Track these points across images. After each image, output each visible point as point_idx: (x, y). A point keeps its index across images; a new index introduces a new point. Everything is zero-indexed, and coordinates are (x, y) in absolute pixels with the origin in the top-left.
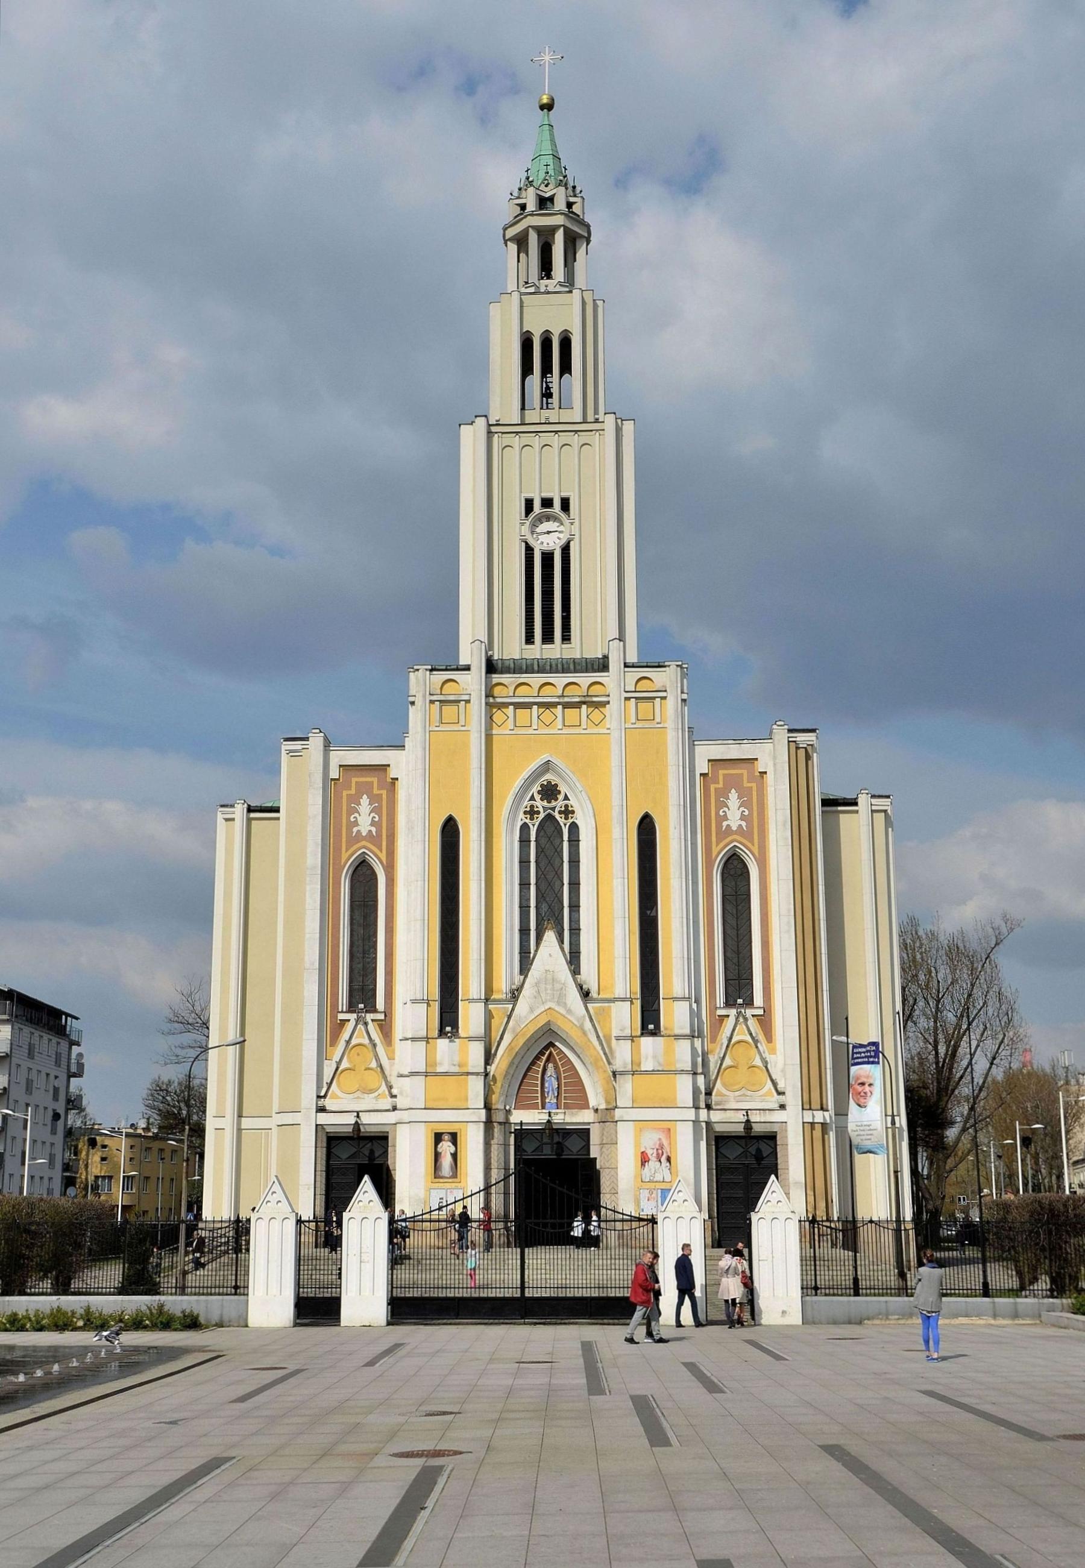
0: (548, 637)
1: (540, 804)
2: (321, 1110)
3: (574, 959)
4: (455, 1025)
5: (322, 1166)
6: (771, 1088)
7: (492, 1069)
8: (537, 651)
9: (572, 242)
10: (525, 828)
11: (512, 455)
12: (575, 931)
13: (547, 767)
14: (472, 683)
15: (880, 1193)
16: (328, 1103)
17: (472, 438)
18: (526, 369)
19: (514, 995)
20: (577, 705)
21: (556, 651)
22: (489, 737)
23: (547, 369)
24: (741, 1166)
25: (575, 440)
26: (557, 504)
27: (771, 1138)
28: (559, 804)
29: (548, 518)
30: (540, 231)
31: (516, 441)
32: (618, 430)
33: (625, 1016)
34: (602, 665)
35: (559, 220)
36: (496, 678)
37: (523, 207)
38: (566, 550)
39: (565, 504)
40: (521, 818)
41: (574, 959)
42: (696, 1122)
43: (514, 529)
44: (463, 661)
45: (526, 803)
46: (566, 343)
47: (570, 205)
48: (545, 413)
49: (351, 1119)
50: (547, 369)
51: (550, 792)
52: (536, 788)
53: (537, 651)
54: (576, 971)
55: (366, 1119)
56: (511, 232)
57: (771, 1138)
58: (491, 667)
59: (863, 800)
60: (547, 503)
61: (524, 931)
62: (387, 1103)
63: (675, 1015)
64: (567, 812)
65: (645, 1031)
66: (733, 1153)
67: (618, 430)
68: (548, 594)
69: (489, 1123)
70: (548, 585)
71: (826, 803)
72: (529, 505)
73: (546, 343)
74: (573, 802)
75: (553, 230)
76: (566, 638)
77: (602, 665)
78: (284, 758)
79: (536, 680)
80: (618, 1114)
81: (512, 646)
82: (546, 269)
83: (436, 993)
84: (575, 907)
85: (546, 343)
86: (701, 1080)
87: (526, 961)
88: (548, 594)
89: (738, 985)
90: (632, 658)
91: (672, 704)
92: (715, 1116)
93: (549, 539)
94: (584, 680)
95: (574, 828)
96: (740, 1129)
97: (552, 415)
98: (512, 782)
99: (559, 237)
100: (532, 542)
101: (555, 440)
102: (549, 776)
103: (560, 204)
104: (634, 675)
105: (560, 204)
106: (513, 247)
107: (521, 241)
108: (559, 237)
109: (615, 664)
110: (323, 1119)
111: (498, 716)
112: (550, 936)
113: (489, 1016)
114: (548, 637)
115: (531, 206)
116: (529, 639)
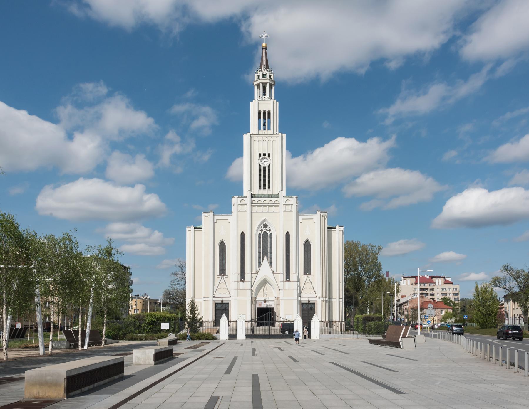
0: (265, 188)
1: (263, 229)
2: (214, 297)
3: (271, 264)
4: (244, 279)
5: (214, 309)
6: (313, 290)
7: (252, 288)
8: (262, 192)
9: (271, 86)
10: (260, 234)
11: (256, 142)
12: (271, 258)
13: (265, 220)
14: (248, 200)
15: (338, 315)
16: (215, 295)
17: (246, 137)
18: (260, 117)
19: (257, 273)
20: (272, 206)
21: (266, 192)
22: (252, 213)
23: (264, 118)
24: (307, 311)
25: (271, 139)
26: (267, 155)
27: (314, 304)
28: (268, 229)
29: (265, 158)
30: (263, 83)
31: (257, 139)
32: (282, 137)
33: (283, 277)
34: (277, 196)
35: (268, 81)
36: (253, 199)
37: (258, 76)
38: (269, 167)
39: (269, 155)
40: (259, 232)
41: (271, 264)
42: (298, 300)
43: (257, 161)
44: (245, 195)
45: (260, 229)
46: (269, 113)
47: (270, 76)
48: (264, 131)
49: (221, 299)
50: (264, 118)
51: (265, 226)
52: (263, 225)
53: (262, 192)
54: (271, 267)
55: (224, 299)
56: (255, 83)
57: (314, 304)
58: (252, 196)
59: (337, 227)
60: (264, 155)
61: (259, 258)
62: (229, 296)
63: (293, 277)
64: (269, 231)
65: (286, 280)
66: (305, 307)
67: (282, 137)
68: (264, 177)
69: (252, 300)
70: (265, 176)
71: (329, 228)
72: (260, 155)
73: (264, 113)
74: (271, 229)
75: (266, 83)
76: (269, 188)
77: (277, 196)
78: (203, 217)
79: (262, 200)
80: (280, 299)
81: (257, 191)
82: (264, 94)
83: (239, 272)
84: (271, 253)
85: (264, 113)
86: (299, 291)
87: (260, 265)
88: (264, 177)
89: (307, 270)
90: (285, 195)
91: (294, 205)
92: (302, 299)
93: (265, 164)
94: (274, 200)
95: (271, 234)
96: (307, 302)
97: (266, 132)
98: (256, 224)
99: (268, 85)
100: (261, 164)
101: (266, 139)
102: (266, 223)
103: (268, 76)
104: (285, 199)
105: (268, 76)
106: (256, 87)
107: (258, 85)
108: (268, 85)
109: (281, 196)
110: (214, 299)
111: (253, 208)
112: (265, 258)
113: (252, 277)
114: (265, 188)
115: (261, 77)
116: (260, 189)
